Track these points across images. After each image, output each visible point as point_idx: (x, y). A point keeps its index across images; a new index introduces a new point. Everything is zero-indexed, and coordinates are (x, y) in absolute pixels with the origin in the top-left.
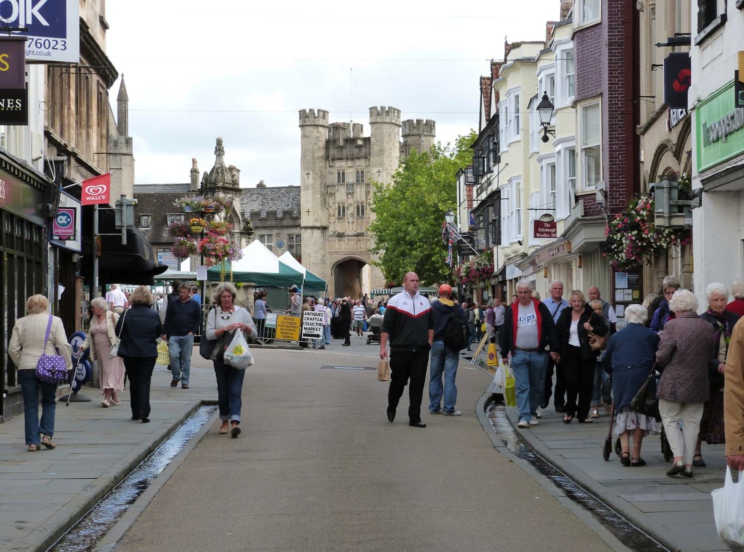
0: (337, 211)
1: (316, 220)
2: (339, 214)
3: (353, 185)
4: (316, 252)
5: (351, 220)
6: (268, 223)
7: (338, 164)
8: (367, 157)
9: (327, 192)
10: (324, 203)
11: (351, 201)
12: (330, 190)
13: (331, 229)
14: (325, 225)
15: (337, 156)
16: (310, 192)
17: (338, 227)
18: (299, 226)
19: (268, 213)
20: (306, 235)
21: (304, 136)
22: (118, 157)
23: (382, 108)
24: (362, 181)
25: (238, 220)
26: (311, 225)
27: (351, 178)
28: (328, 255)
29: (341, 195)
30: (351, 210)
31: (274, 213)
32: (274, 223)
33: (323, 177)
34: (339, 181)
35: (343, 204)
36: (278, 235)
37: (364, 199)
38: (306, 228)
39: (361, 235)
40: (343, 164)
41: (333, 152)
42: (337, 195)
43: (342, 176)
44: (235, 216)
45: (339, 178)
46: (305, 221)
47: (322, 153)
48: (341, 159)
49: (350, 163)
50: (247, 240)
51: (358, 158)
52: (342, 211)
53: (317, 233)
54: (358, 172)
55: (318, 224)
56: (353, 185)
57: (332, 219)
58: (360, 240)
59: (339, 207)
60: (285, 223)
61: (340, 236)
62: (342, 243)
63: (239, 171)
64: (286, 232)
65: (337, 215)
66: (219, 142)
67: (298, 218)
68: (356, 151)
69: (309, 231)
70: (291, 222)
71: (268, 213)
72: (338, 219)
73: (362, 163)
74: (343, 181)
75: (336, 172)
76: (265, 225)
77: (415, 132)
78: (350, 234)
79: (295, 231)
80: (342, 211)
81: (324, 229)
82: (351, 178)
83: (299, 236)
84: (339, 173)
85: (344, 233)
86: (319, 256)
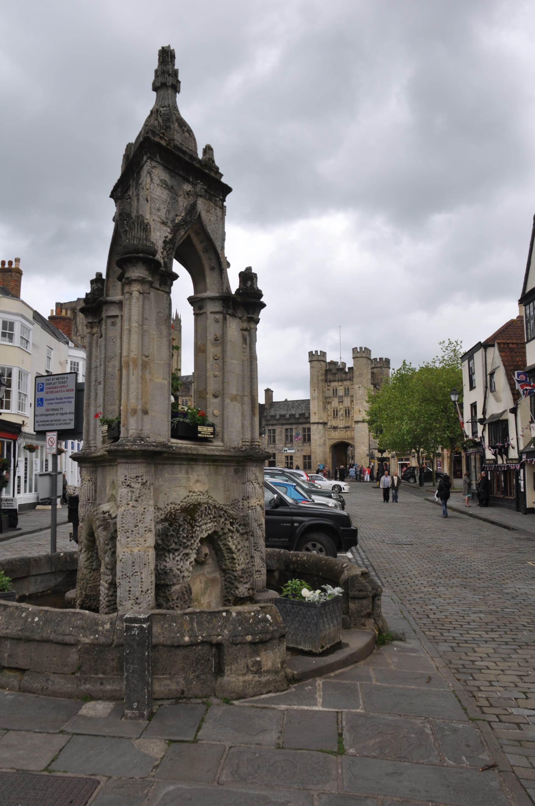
0: (332, 413)
1: (320, 419)
2: (334, 415)
3: (342, 397)
4: (320, 438)
5: (341, 418)
6: (290, 421)
7: (333, 384)
8: (351, 379)
9: (326, 401)
10: (325, 408)
11: (341, 406)
12: (328, 400)
13: (329, 424)
14: (325, 422)
15: (332, 379)
16: (316, 401)
17: (333, 423)
18: (309, 423)
19: (290, 415)
20: (313, 428)
21: (312, 367)
23: (361, 348)
24: (348, 394)
25: (214, 263)
26: (317, 421)
27: (341, 393)
28: (327, 440)
29: (335, 403)
30: (342, 412)
31: (294, 415)
32: (294, 421)
33: (323, 392)
34: (334, 395)
35: (337, 408)
36: (296, 428)
37: (349, 405)
38: (314, 423)
39: (348, 427)
40: (335, 384)
41: (330, 377)
42: (333, 403)
43: (335, 391)
44: (206, 251)
45: (334, 392)
46: (313, 419)
47: (323, 377)
48: (335, 381)
49: (340, 383)
50: (245, 325)
51: (345, 380)
52: (335, 413)
53: (321, 427)
54: (345, 389)
55: (321, 421)
56: (342, 397)
57: (330, 418)
58: (347, 431)
59: (334, 410)
60: (300, 421)
61: (335, 428)
62: (336, 432)
63: (272, 392)
64: (301, 427)
65: (332, 416)
66: (166, 56)
67: (309, 418)
68: (344, 376)
69: (316, 425)
70: (304, 421)
72: (334, 418)
73: (348, 383)
74: (336, 394)
75: (332, 389)
77: (378, 365)
78: (341, 427)
79: (306, 426)
80: (335, 413)
81: (325, 424)
82: (341, 393)
83: (309, 429)
84: (333, 390)
85: (337, 427)
86: (322, 440)
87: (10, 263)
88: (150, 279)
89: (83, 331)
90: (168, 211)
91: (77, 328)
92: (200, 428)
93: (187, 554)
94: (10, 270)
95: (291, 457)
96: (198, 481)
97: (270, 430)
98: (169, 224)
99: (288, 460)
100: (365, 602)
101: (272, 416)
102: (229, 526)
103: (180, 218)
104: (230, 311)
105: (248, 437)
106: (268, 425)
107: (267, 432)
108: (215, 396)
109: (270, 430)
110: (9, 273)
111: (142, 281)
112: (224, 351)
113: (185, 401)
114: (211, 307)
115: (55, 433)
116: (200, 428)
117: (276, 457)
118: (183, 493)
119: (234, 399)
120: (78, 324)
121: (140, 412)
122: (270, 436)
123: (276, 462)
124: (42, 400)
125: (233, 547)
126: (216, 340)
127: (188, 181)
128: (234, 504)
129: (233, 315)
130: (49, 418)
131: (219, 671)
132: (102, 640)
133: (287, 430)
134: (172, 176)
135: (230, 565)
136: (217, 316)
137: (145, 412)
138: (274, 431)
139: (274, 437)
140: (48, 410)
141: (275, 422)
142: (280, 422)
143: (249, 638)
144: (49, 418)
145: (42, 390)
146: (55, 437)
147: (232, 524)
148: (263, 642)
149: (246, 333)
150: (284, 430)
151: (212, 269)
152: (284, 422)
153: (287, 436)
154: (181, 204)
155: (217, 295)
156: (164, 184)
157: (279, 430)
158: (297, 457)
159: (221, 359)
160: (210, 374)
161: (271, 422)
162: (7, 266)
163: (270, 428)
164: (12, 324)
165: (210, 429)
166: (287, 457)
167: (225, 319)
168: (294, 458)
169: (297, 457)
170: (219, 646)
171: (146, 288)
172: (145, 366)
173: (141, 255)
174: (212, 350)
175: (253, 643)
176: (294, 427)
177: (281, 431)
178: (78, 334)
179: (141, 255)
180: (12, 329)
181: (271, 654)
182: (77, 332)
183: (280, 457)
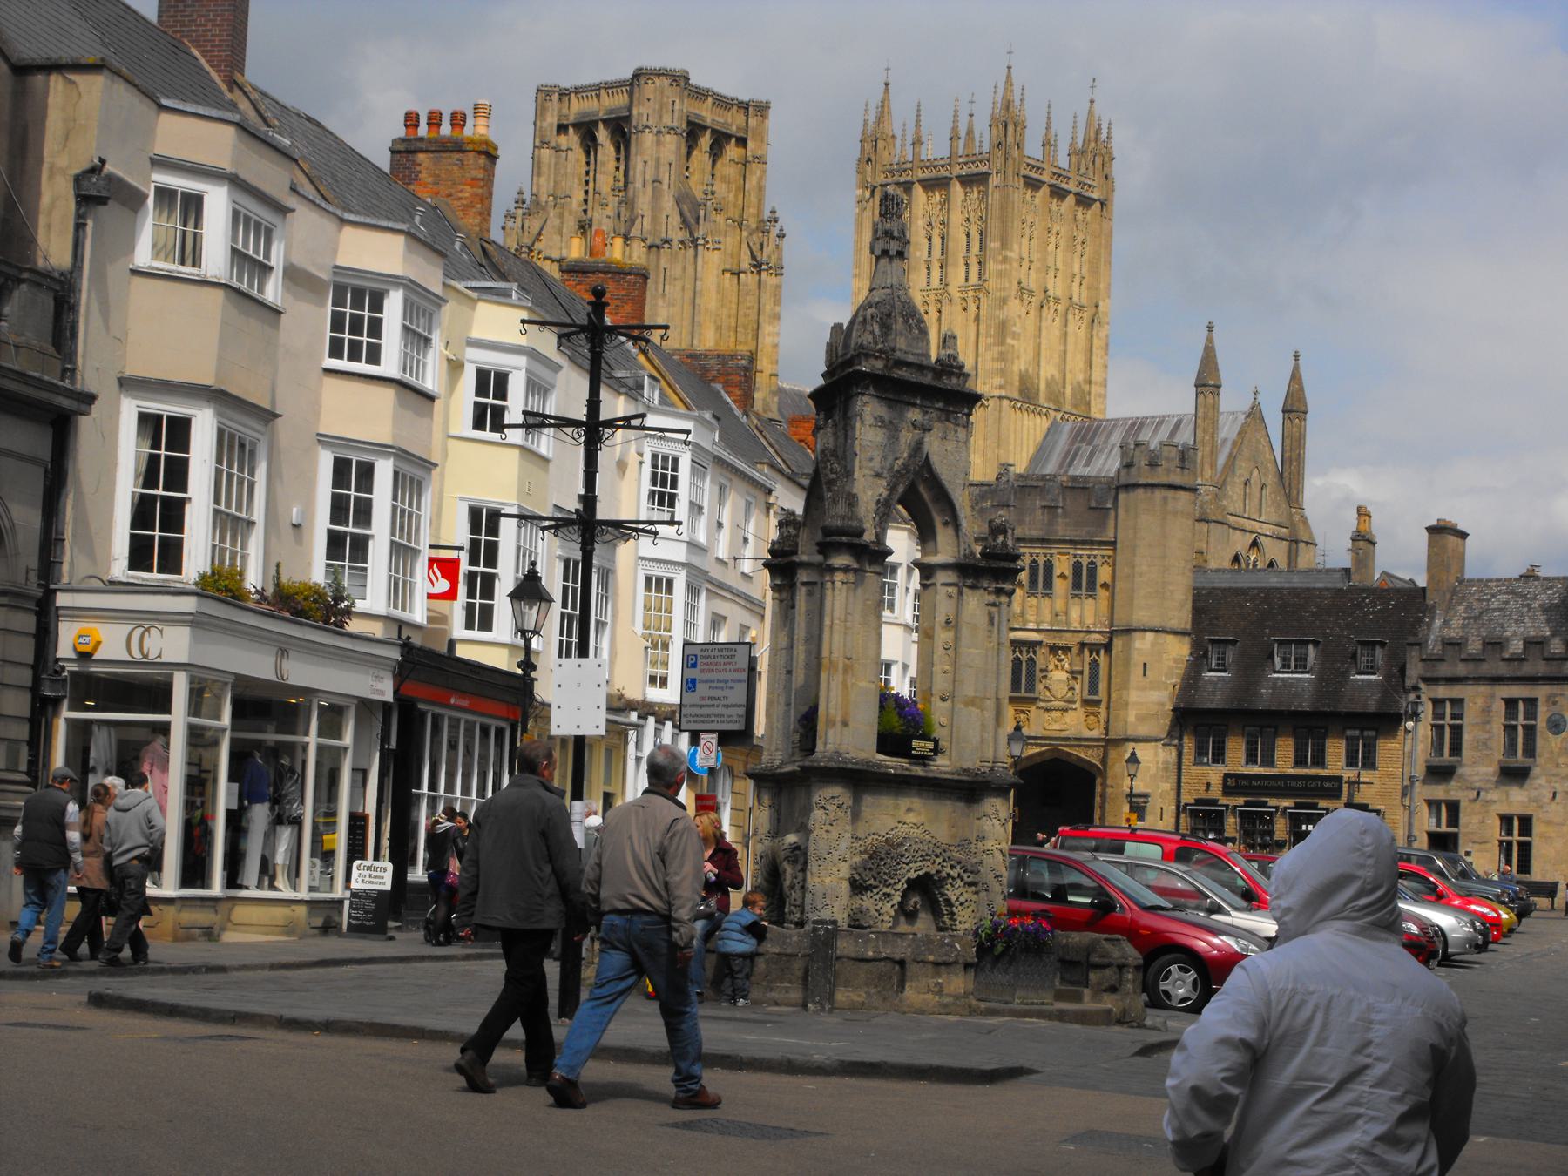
6: (1527, 669)
22: (1159, 494)
32: (1541, 668)
50: (992, 598)
71: (1529, 643)
76: (1519, 674)
87: (458, 120)
88: (856, 566)
89: (654, 219)
90: (885, 458)
91: (629, 203)
92: (915, 743)
93: (889, 895)
94: (457, 147)
95: (1526, 823)
96: (909, 810)
97: (1437, 703)
98: (885, 474)
99: (1509, 833)
100: (1108, 972)
101: (1449, 643)
102: (948, 870)
103: (900, 462)
104: (969, 582)
105: (990, 755)
106: (1431, 681)
107: (1427, 710)
108: (944, 700)
109: (1437, 703)
110: (456, 156)
111: (846, 569)
112: (957, 639)
113: (1085, 561)
114: (942, 577)
115: (715, 735)
116: (915, 743)
117: (1463, 819)
118: (892, 823)
119: (971, 702)
120: (638, 185)
121: (839, 725)
122: (1439, 729)
123: (1461, 841)
124: (693, 681)
125: (953, 898)
126: (948, 622)
127: (914, 405)
128: (964, 844)
129: (973, 587)
130: (705, 711)
131: (902, 986)
132: (789, 951)
133: (1511, 703)
134: (889, 407)
135: (948, 922)
136: (950, 589)
137: (845, 724)
138: (1457, 702)
139: (1457, 731)
140: (703, 698)
141: (1462, 670)
142: (1485, 669)
143: (931, 958)
144: (705, 711)
145: (694, 666)
146: (714, 742)
147: (952, 867)
148: (946, 964)
149: (994, 609)
150: (1500, 707)
151: (946, 524)
152: (1503, 670)
153: (1510, 730)
154: (902, 440)
155: (951, 560)
156: (881, 422)
157: (1480, 701)
158: (1549, 823)
159: (954, 648)
160: (937, 669)
161: (1443, 670)
162: (446, 129)
163: (1442, 691)
164: (502, 379)
165: (930, 745)
166: (1506, 820)
167: (960, 593)
168: (1537, 828)
169: (1549, 823)
170: (902, 963)
171: (851, 577)
172: (847, 670)
173: (844, 539)
174: (943, 636)
175: (936, 964)
176: (1541, 692)
177: (1487, 710)
178: (635, 232)
179: (844, 539)
180: (501, 393)
181: (953, 978)
182: (631, 222)
183: (1475, 820)
